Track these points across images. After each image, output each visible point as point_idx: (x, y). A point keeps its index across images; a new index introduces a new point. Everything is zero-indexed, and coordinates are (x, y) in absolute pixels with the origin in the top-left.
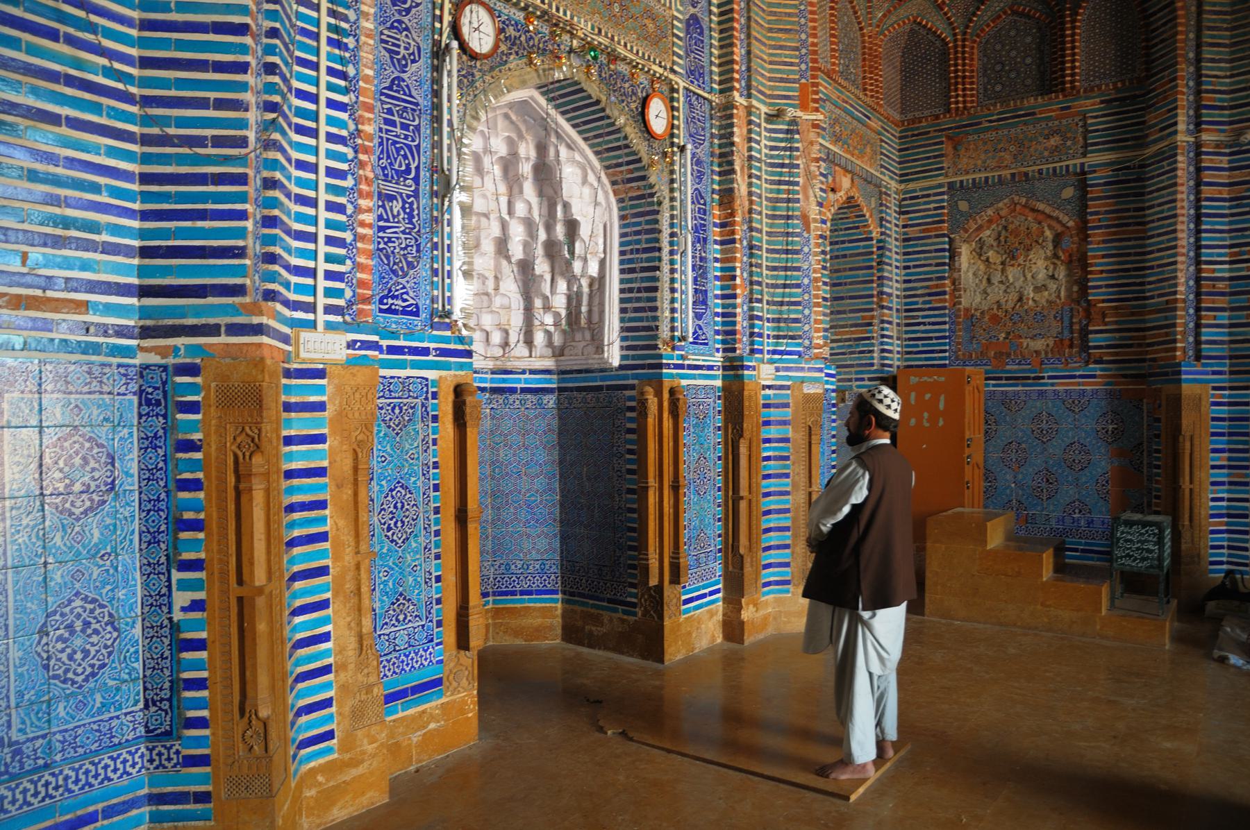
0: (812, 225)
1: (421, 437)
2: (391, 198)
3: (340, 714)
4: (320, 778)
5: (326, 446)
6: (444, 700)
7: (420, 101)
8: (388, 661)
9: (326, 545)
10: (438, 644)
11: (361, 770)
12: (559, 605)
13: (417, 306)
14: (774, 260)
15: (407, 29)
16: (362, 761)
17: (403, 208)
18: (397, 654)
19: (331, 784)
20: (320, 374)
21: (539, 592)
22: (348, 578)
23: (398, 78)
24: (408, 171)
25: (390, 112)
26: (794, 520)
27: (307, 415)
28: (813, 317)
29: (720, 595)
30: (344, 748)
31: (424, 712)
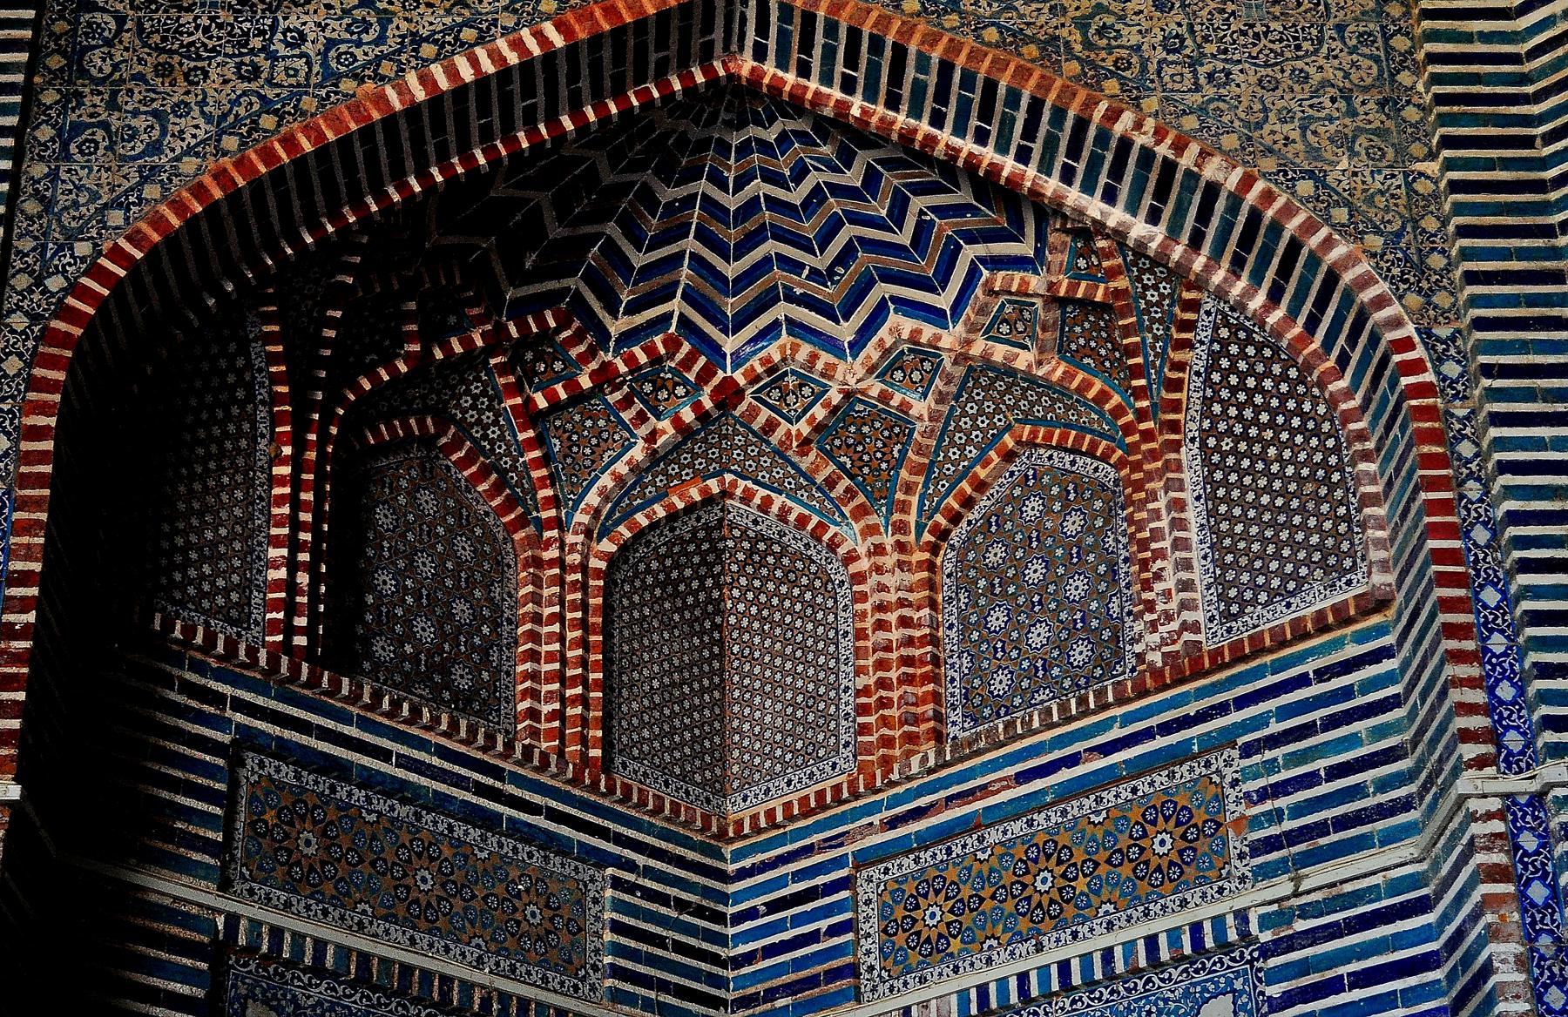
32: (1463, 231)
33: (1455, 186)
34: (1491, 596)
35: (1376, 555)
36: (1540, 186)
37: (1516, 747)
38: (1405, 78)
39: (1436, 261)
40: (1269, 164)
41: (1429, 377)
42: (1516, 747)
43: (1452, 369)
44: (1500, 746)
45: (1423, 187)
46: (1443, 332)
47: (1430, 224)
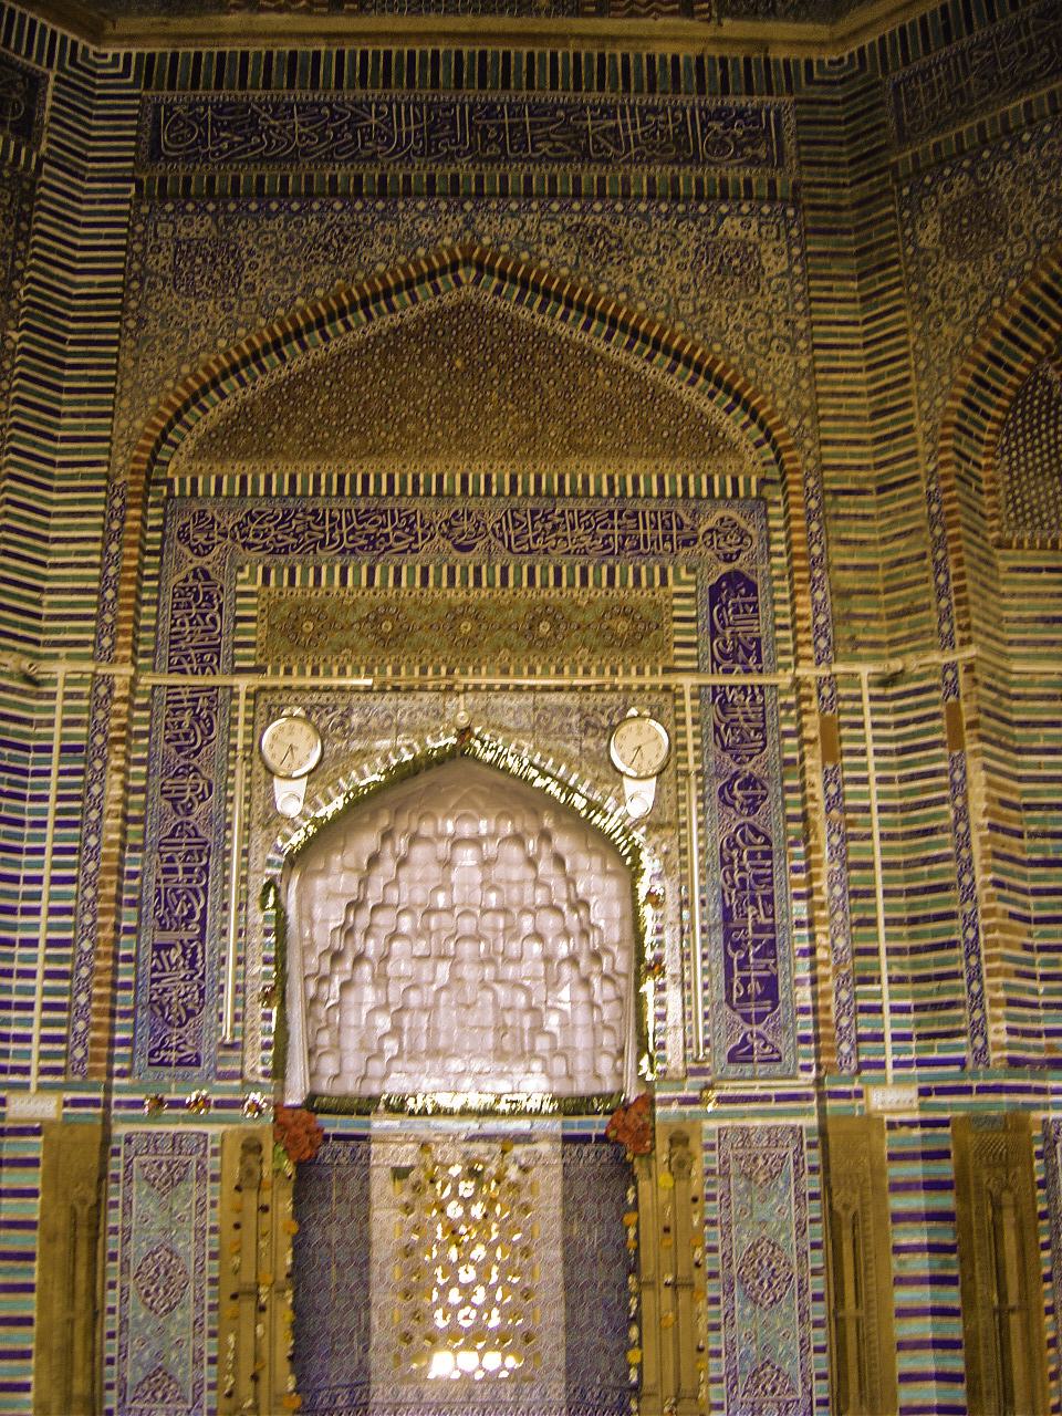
2: (169, 947)
7: (209, 838)
14: (897, 908)
17: (184, 955)
24: (191, 914)
25: (170, 860)
26: (970, 1362)
32: (22, 376)
33: (24, 351)
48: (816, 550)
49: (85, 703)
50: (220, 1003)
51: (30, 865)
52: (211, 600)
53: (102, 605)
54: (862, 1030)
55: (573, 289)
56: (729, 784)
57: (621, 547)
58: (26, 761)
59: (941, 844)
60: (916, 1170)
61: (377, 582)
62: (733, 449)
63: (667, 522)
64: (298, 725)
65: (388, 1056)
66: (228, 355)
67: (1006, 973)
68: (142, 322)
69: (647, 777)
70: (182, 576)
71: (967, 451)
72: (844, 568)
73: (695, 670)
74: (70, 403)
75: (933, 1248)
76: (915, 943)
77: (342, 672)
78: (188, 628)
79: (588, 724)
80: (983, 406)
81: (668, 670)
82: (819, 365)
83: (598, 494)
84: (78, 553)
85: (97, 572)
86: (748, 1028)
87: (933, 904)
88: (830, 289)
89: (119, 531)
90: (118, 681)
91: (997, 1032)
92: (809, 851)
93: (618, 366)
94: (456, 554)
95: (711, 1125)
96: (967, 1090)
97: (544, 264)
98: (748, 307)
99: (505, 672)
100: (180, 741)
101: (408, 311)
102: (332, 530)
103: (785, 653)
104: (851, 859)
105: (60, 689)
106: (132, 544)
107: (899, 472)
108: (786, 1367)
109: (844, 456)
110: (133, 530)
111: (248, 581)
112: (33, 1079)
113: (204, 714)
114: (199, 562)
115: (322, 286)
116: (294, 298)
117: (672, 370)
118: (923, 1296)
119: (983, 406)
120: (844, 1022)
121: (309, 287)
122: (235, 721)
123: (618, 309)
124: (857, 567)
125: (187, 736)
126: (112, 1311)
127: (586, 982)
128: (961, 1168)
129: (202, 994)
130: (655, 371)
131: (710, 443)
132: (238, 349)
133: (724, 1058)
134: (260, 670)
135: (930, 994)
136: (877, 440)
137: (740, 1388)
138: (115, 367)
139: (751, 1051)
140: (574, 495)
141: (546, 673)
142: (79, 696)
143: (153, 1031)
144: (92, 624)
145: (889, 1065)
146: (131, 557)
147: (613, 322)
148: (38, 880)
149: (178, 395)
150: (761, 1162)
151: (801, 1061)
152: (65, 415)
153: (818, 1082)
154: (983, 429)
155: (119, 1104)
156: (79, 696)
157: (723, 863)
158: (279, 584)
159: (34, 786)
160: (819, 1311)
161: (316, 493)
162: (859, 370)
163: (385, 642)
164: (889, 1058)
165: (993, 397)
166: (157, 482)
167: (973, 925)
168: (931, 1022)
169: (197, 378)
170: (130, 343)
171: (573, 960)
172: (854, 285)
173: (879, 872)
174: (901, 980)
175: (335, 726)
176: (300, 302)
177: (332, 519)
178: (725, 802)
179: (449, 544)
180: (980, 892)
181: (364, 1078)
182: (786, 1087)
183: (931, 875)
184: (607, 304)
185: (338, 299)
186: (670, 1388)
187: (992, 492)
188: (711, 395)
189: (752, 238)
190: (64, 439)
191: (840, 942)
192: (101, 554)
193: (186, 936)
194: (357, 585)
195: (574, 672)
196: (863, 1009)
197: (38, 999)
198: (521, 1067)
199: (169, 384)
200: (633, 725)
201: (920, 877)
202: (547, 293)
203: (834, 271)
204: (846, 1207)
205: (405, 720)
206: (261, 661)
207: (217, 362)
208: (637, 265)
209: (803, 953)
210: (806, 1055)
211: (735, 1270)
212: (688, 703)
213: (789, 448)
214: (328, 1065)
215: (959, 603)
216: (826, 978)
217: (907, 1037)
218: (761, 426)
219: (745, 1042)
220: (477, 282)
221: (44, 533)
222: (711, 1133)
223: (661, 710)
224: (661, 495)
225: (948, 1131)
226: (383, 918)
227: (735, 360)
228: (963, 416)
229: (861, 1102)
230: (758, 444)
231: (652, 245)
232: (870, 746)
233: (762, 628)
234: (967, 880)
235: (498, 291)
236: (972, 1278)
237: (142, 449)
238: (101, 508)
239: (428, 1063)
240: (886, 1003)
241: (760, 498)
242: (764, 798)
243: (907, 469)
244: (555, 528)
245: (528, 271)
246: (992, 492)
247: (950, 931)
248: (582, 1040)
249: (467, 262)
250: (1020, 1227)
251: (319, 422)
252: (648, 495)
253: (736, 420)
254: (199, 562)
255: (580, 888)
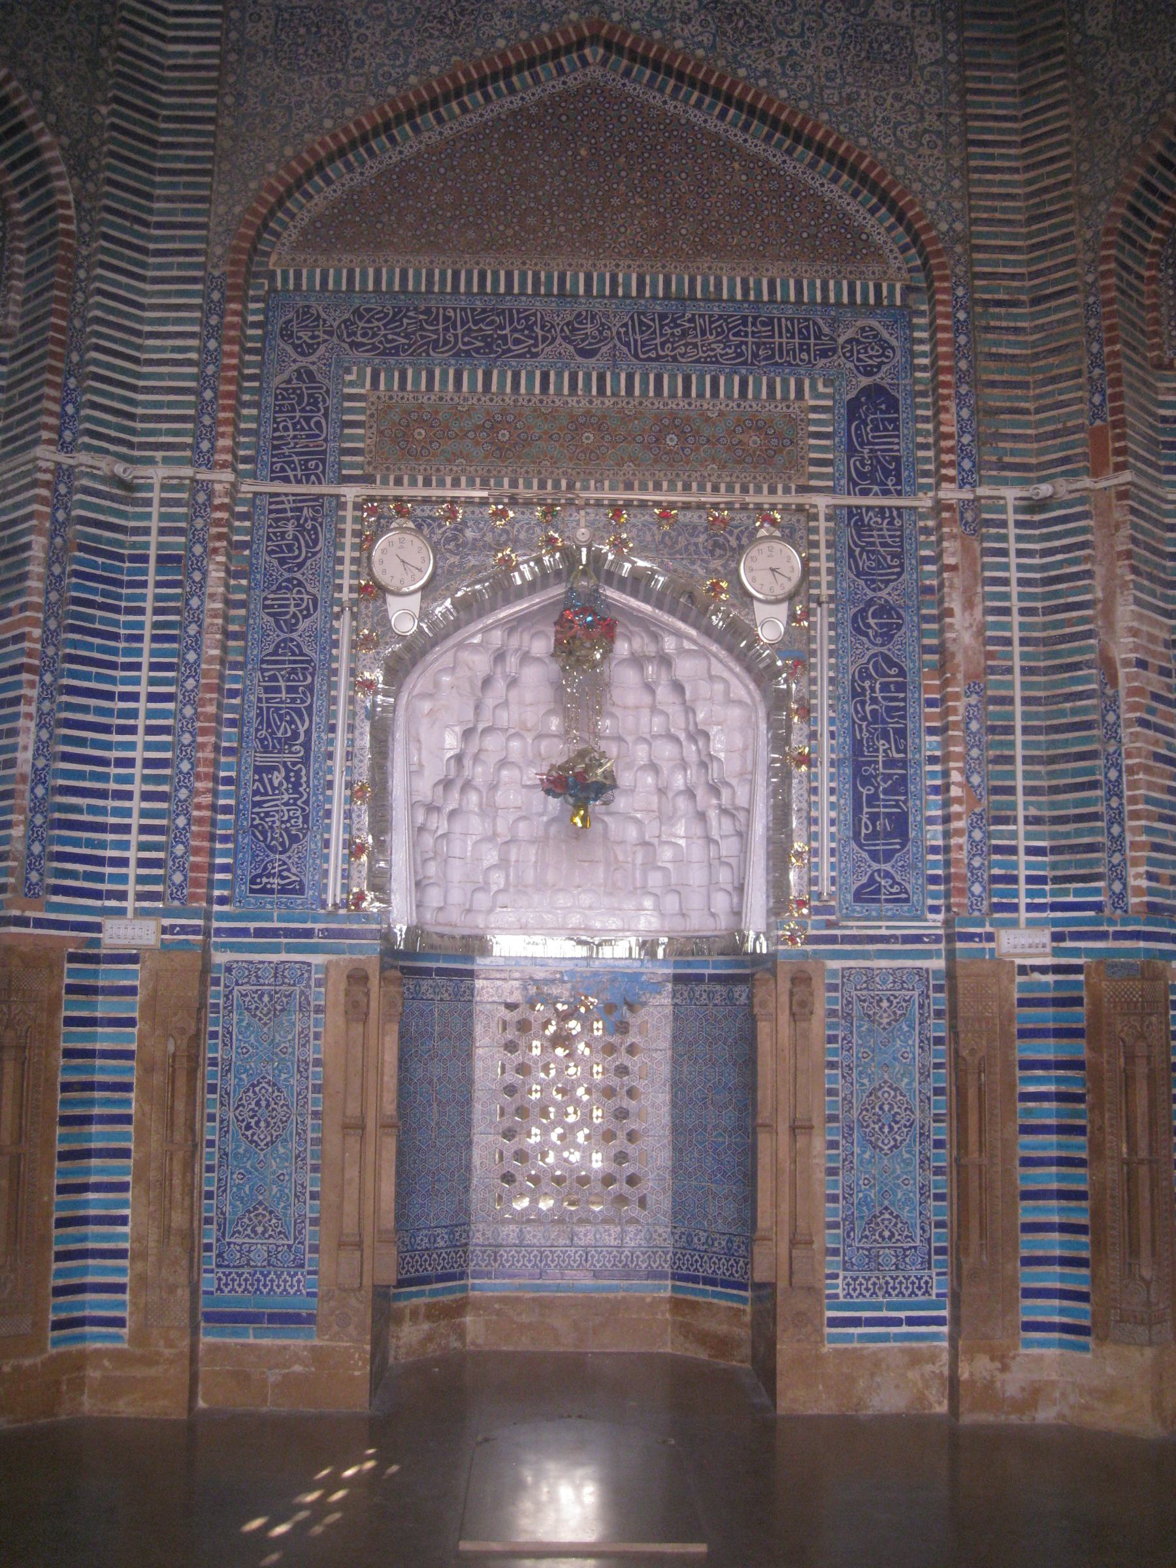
0: (1122, 672)
1: (298, 1029)
2: (271, 769)
3: (134, 1304)
4: (106, 1363)
5: (135, 1030)
6: (316, 1342)
8: (240, 1275)
9: (130, 1128)
10: (309, 1273)
11: (152, 1372)
12: (748, 1308)
13: (301, 882)
14: (1037, 745)
15: (300, 584)
16: (157, 1363)
17: (287, 778)
18: (251, 1270)
19: (118, 1373)
20: (134, 959)
21: (725, 1284)
22: (153, 1165)
23: (284, 640)
24: (295, 735)
25: (274, 678)
26: (1096, 1213)
27: (115, 999)
28: (1129, 837)
29: (945, 1329)
30: (135, 1339)
31: (285, 1348)
33: (114, 127)
34: (75, 357)
35: (13, 308)
36: (153, 143)
37: (68, 439)
38: (104, 52)
39: (93, 164)
40: (22, 73)
41: (73, 227)
42: (68, 439)
43: (86, 227)
44: (60, 437)
45: (97, 119)
46: (86, 205)
47: (95, 142)
48: (963, 365)
49: (183, 510)
50: (328, 828)
51: (125, 681)
52: (316, 404)
53: (202, 407)
54: (996, 871)
55: (710, 73)
56: (863, 611)
57: (755, 355)
58: (120, 570)
59: (1086, 680)
60: (1047, 1016)
61: (494, 388)
62: (876, 254)
63: (804, 330)
64: (408, 537)
65: (494, 888)
66: (335, 137)
67: (1149, 816)
68: (240, 96)
69: (777, 601)
70: (285, 376)
71: (1130, 262)
72: (993, 384)
73: (831, 490)
74: (163, 186)
75: (1060, 1097)
76: (1054, 782)
77: (456, 484)
78: (291, 433)
79: (716, 545)
80: (1149, 213)
81: (803, 489)
82: (973, 163)
83: (732, 299)
84: (175, 349)
85: (195, 370)
86: (875, 866)
87: (1074, 742)
88: (986, 80)
89: (218, 328)
90: (218, 487)
91: (1136, 877)
92: (946, 683)
93: (755, 158)
94: (579, 359)
95: (834, 964)
96: (1103, 936)
97: (679, 44)
98: (898, 98)
99: (629, 487)
100: (285, 555)
101: (528, 92)
102: (446, 329)
103: (926, 474)
104: (990, 693)
105: (156, 495)
106: (231, 341)
107: (1056, 282)
108: (905, 1214)
109: (996, 263)
110: (232, 326)
111: (359, 384)
112: (130, 904)
113: (309, 525)
114: (303, 362)
115: (436, 63)
116: (406, 75)
117: (813, 165)
118: (1049, 1145)
119: (1149, 213)
120: (977, 862)
121: (423, 63)
122: (341, 533)
123: (758, 96)
124: (1007, 384)
125: (290, 548)
126: (211, 1144)
127: (702, 816)
128: (1095, 1014)
129: (306, 821)
130: (795, 165)
131: (850, 247)
132: (346, 130)
133: (850, 897)
134: (368, 479)
135: (1066, 835)
136: (1033, 248)
137: (858, 1233)
138: (212, 147)
139: (877, 891)
140: (706, 299)
141: (672, 488)
142: (178, 503)
143: (254, 856)
144: (190, 426)
145: (1022, 908)
146: (231, 355)
147: (752, 110)
148: (134, 697)
149: (280, 180)
150: (885, 1004)
151: (930, 902)
152: (159, 199)
153: (947, 923)
154: (1147, 238)
155: (219, 932)
156: (178, 503)
157: (855, 694)
158: (389, 388)
159: (130, 598)
160: (943, 1157)
161: (429, 291)
162: (1015, 170)
163: (501, 452)
164: (1023, 901)
165: (1161, 204)
166: (257, 275)
167: (1117, 766)
168: (1068, 864)
169: (302, 162)
170: (228, 122)
171: (690, 793)
172: (1014, 76)
173: (1018, 708)
174: (1037, 820)
175: (448, 541)
176: (413, 79)
177: (447, 319)
178: (858, 630)
179: (572, 349)
180: (1124, 733)
181: (469, 911)
182: (911, 927)
183: (1074, 712)
184: (746, 90)
185: (454, 78)
186: (786, 1229)
187: (1155, 307)
188: (855, 195)
189: (905, 21)
190: (159, 226)
191: (976, 780)
192: (198, 350)
193: (288, 758)
194: (473, 390)
195: (702, 488)
196: (998, 850)
197: (135, 821)
198: (630, 905)
199: (271, 167)
200: (764, 546)
201: (1062, 713)
202: (680, 76)
203: (993, 60)
204: (973, 1052)
205: (523, 536)
206: (370, 470)
207: (323, 144)
208: (780, 47)
209: (936, 790)
210: (934, 895)
211: (855, 1113)
212: (822, 524)
213: (938, 253)
214: (434, 897)
215: (1115, 425)
216: (959, 816)
217: (1042, 880)
218: (908, 229)
219: (872, 881)
220: (604, 62)
221: (138, 326)
222: (834, 973)
223: (793, 531)
224: (799, 301)
225: (1081, 977)
226: (492, 743)
227: (882, 156)
228: (1127, 223)
229: (992, 945)
230: (904, 249)
231: (796, 25)
232: (1014, 575)
233: (902, 448)
234: (1111, 717)
235: (627, 73)
236: (1101, 1129)
237: (243, 237)
238: (199, 301)
239: (536, 898)
240: (1022, 844)
241: (905, 305)
242: (899, 627)
243: (1064, 279)
244: (685, 333)
245: (661, 52)
246: (1155, 307)
247: (1091, 771)
248: (697, 876)
249: (594, 40)
250: (1151, 1077)
251: (432, 212)
252: (785, 301)
253: (881, 221)
254: (303, 362)
255: (701, 716)
